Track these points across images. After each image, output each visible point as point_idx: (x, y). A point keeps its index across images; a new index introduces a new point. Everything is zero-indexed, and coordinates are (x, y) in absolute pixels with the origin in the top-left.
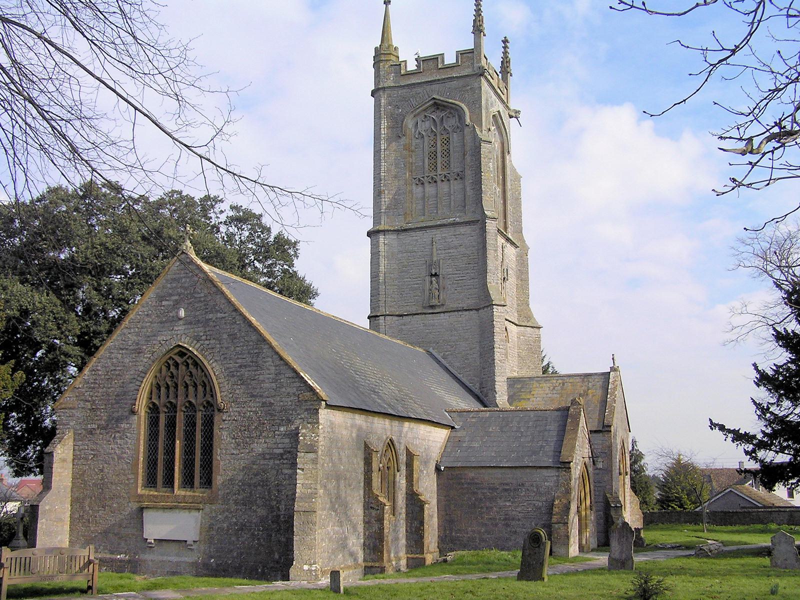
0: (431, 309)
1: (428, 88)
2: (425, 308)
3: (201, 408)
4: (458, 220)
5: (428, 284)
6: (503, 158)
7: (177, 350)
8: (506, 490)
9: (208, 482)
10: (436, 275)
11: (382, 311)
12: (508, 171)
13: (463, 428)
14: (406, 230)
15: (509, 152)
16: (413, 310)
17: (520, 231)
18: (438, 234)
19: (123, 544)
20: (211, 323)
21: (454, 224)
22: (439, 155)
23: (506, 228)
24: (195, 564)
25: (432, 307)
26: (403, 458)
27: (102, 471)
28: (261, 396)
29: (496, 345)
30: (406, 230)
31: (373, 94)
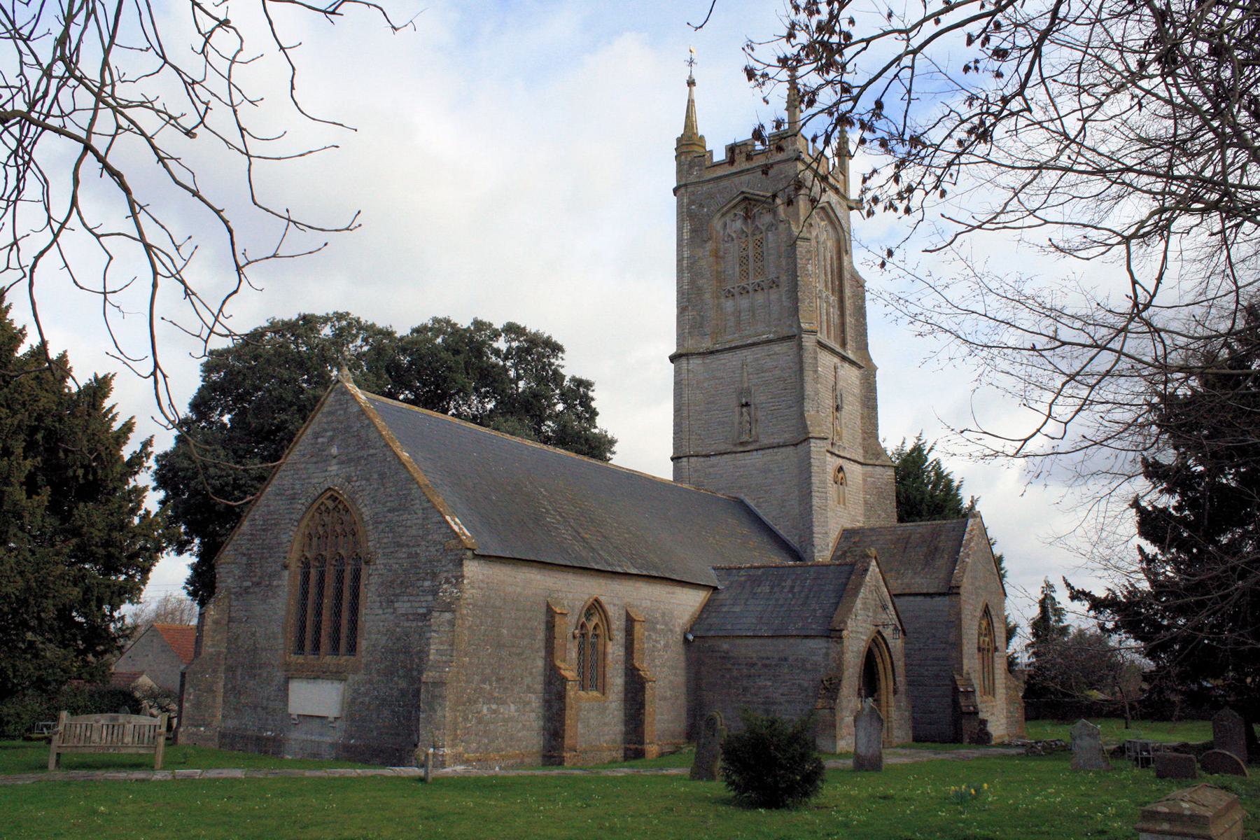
0: (743, 446)
1: (736, 180)
2: (735, 445)
3: (351, 562)
4: (771, 336)
5: (737, 414)
6: (840, 259)
7: (329, 494)
8: (765, 666)
9: (352, 648)
10: (747, 405)
11: (686, 450)
12: (847, 275)
13: (727, 588)
14: (712, 353)
15: (847, 252)
16: (722, 448)
17: (863, 346)
18: (748, 354)
19: (270, 721)
20: (363, 462)
21: (769, 342)
22: (751, 260)
23: (844, 345)
24: (333, 745)
25: (742, 444)
26: (618, 624)
27: (253, 634)
28: (408, 546)
29: (814, 488)
30: (712, 353)
31: (675, 191)
